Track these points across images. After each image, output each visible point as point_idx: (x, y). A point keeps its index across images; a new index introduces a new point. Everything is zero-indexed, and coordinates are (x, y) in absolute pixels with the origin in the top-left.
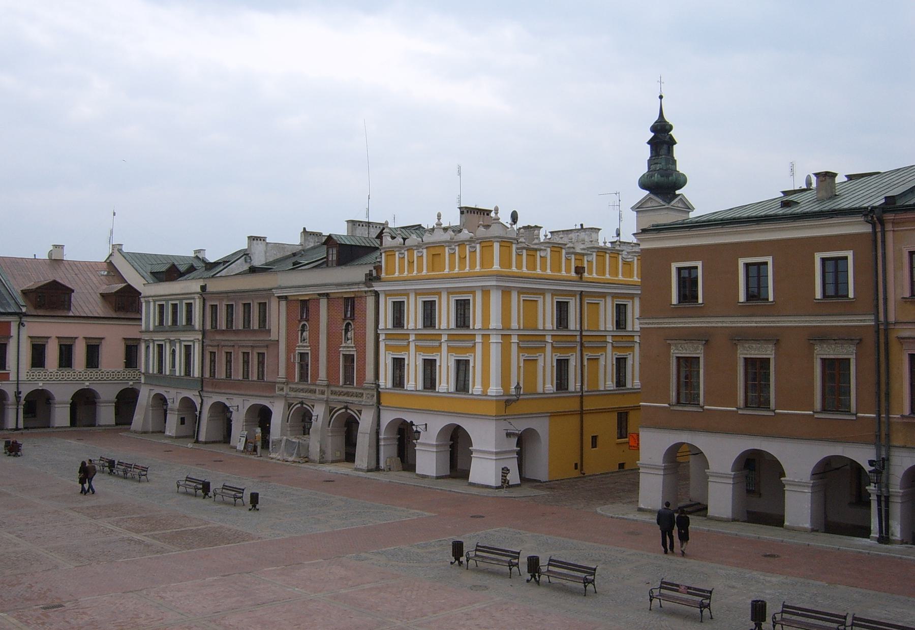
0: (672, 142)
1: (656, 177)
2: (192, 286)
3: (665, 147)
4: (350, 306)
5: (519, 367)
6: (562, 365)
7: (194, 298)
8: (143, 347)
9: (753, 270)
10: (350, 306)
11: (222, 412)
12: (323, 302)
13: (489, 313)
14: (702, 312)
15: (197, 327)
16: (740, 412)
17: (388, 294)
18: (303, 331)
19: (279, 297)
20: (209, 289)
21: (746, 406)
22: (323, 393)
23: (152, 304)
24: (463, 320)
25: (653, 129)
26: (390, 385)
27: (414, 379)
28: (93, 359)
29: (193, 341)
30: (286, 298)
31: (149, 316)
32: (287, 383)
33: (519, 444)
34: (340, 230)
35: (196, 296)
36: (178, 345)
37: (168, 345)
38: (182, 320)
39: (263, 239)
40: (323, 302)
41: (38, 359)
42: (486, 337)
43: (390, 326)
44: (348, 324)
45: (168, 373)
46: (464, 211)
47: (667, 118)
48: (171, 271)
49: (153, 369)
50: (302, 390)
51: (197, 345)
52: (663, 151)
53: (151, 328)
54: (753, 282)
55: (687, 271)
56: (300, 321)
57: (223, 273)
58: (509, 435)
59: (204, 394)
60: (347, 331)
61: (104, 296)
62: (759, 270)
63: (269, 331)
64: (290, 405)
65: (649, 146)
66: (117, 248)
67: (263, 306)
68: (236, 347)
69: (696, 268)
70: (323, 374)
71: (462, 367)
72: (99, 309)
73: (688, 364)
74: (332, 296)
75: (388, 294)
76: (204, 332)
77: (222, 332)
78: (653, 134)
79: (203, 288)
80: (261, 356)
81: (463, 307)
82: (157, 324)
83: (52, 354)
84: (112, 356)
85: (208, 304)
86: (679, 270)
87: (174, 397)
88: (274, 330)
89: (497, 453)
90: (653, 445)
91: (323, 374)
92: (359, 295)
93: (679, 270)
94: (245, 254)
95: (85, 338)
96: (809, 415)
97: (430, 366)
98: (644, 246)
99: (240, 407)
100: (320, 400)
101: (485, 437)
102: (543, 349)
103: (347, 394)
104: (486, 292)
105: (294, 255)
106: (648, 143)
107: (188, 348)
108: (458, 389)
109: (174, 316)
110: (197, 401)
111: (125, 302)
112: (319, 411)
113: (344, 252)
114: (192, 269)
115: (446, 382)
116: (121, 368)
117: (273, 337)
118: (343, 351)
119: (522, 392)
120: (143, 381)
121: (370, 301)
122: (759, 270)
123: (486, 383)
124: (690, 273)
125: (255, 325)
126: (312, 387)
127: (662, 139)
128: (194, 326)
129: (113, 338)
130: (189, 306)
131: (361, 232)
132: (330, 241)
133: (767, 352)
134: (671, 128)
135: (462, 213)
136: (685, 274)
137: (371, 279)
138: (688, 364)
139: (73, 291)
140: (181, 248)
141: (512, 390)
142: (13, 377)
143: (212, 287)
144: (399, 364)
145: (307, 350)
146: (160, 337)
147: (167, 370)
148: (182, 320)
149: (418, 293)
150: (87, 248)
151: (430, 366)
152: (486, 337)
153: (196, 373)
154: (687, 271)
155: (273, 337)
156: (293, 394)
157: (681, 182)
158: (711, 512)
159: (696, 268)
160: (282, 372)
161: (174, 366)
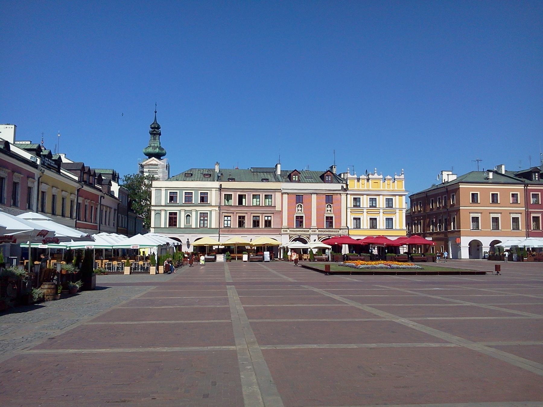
4: (329, 198)
8: (153, 213)
10: (329, 198)
12: (314, 197)
15: (213, 204)
23: (163, 192)
29: (211, 211)
36: (194, 213)
37: (183, 213)
51: (214, 213)
68: (249, 214)
70: (314, 224)
75: (351, 195)
76: (220, 207)
91: (314, 224)
117: (278, 208)
133: (498, 216)
144: (357, 220)
155: (278, 208)
160: (285, 224)
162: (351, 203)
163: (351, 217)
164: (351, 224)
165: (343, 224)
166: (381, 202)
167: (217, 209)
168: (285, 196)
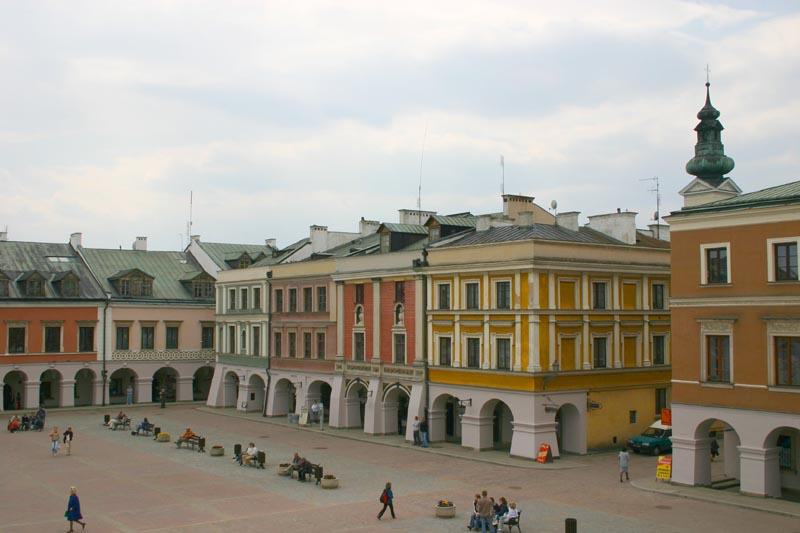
0: (719, 127)
1: (704, 163)
2: (258, 273)
3: (712, 132)
5: (557, 346)
6: (599, 345)
7: (260, 284)
8: (217, 328)
9: (782, 251)
11: (287, 387)
12: (376, 287)
13: (529, 294)
14: (731, 292)
16: (771, 389)
17: (434, 278)
18: (358, 313)
19: (337, 282)
20: (275, 275)
21: (777, 384)
22: (377, 370)
23: (224, 289)
24: (503, 302)
25: (700, 116)
26: (437, 363)
27: (459, 357)
28: (172, 342)
30: (343, 282)
31: (222, 300)
32: (344, 361)
33: (559, 417)
34: (392, 218)
35: (263, 282)
38: (251, 304)
39: (324, 229)
40: (376, 287)
41: (123, 342)
42: (525, 317)
43: (436, 307)
44: (399, 306)
45: (239, 352)
46: (507, 198)
47: (714, 104)
48: (241, 259)
49: (226, 349)
50: (358, 368)
52: (710, 137)
53: (224, 312)
54: (783, 264)
55: (715, 253)
56: (356, 304)
57: (288, 260)
58: (548, 410)
59: (271, 371)
60: (398, 312)
61: (184, 283)
62: (788, 251)
63: (328, 314)
64: (347, 381)
65: (696, 132)
66: (195, 239)
67: (322, 291)
69: (725, 249)
70: (376, 353)
71: (503, 345)
72: (180, 294)
73: (717, 343)
74: (384, 280)
75: (434, 278)
76: (270, 316)
77: (288, 315)
78: (700, 121)
79: (269, 274)
80: (321, 336)
81: (503, 289)
82: (229, 307)
83: (135, 335)
84: (190, 338)
85: (273, 289)
86: (708, 251)
87: (245, 373)
88: (332, 312)
89: (536, 427)
90: (685, 423)
91: (376, 353)
92: (408, 278)
93: (708, 251)
94: (307, 242)
95: (140, 321)
96: (766, 390)
97: (473, 345)
98: (674, 228)
99: (303, 381)
100: (375, 376)
101: (525, 409)
102: (580, 329)
103: (399, 371)
104: (524, 275)
105: (353, 242)
106: (695, 130)
107: (256, 330)
108: (499, 368)
109: (244, 299)
110: (265, 378)
111: (199, 288)
112: (373, 387)
113: (400, 240)
114: (262, 256)
115: (488, 360)
116: (198, 348)
117: (332, 319)
118: (395, 331)
119: (560, 369)
120: (217, 360)
121: (419, 285)
122: (788, 251)
123: (525, 362)
124: (718, 255)
125: (315, 308)
126: (368, 365)
127: (709, 124)
128: (261, 310)
129: (190, 321)
130: (257, 291)
131: (414, 220)
132: (382, 228)
134: (718, 114)
135: (505, 200)
136: (714, 255)
137: (417, 264)
138: (717, 343)
139: (153, 278)
140: (252, 238)
141: (551, 369)
142: (100, 357)
143: (278, 273)
145: (362, 331)
146: (232, 320)
147: (238, 350)
148: (251, 304)
149: (462, 277)
150: (167, 240)
151: (473, 345)
152: (525, 317)
153: (264, 352)
154: (715, 253)
155: (332, 319)
156: (350, 371)
157: (728, 166)
158: (743, 488)
159: (725, 249)
160: (340, 351)
161: (244, 346)
162: (434, 303)
163: (434, 340)
164: (434, 358)
165: (419, 354)
166: (488, 298)
167: (267, 320)
168: (341, 287)
